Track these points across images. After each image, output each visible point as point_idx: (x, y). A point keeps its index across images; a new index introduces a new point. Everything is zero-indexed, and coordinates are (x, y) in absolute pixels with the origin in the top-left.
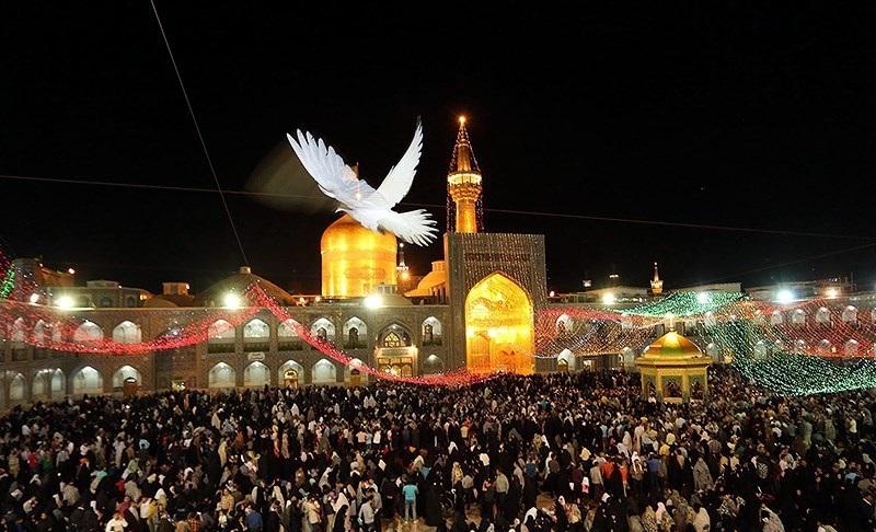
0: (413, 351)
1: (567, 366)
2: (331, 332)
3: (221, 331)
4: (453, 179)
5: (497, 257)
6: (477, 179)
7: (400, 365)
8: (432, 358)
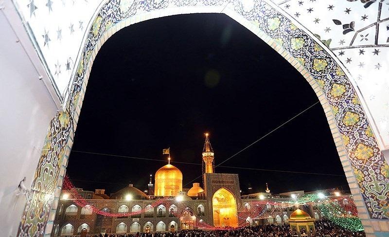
2: (164, 210)
3: (123, 209)
4: (204, 154)
5: (223, 182)
6: (213, 154)
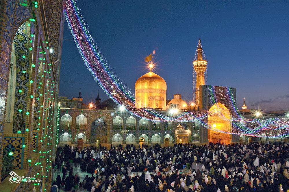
0: (189, 132)
1: (242, 140)
3: (118, 120)
7: (184, 137)
8: (196, 135)
